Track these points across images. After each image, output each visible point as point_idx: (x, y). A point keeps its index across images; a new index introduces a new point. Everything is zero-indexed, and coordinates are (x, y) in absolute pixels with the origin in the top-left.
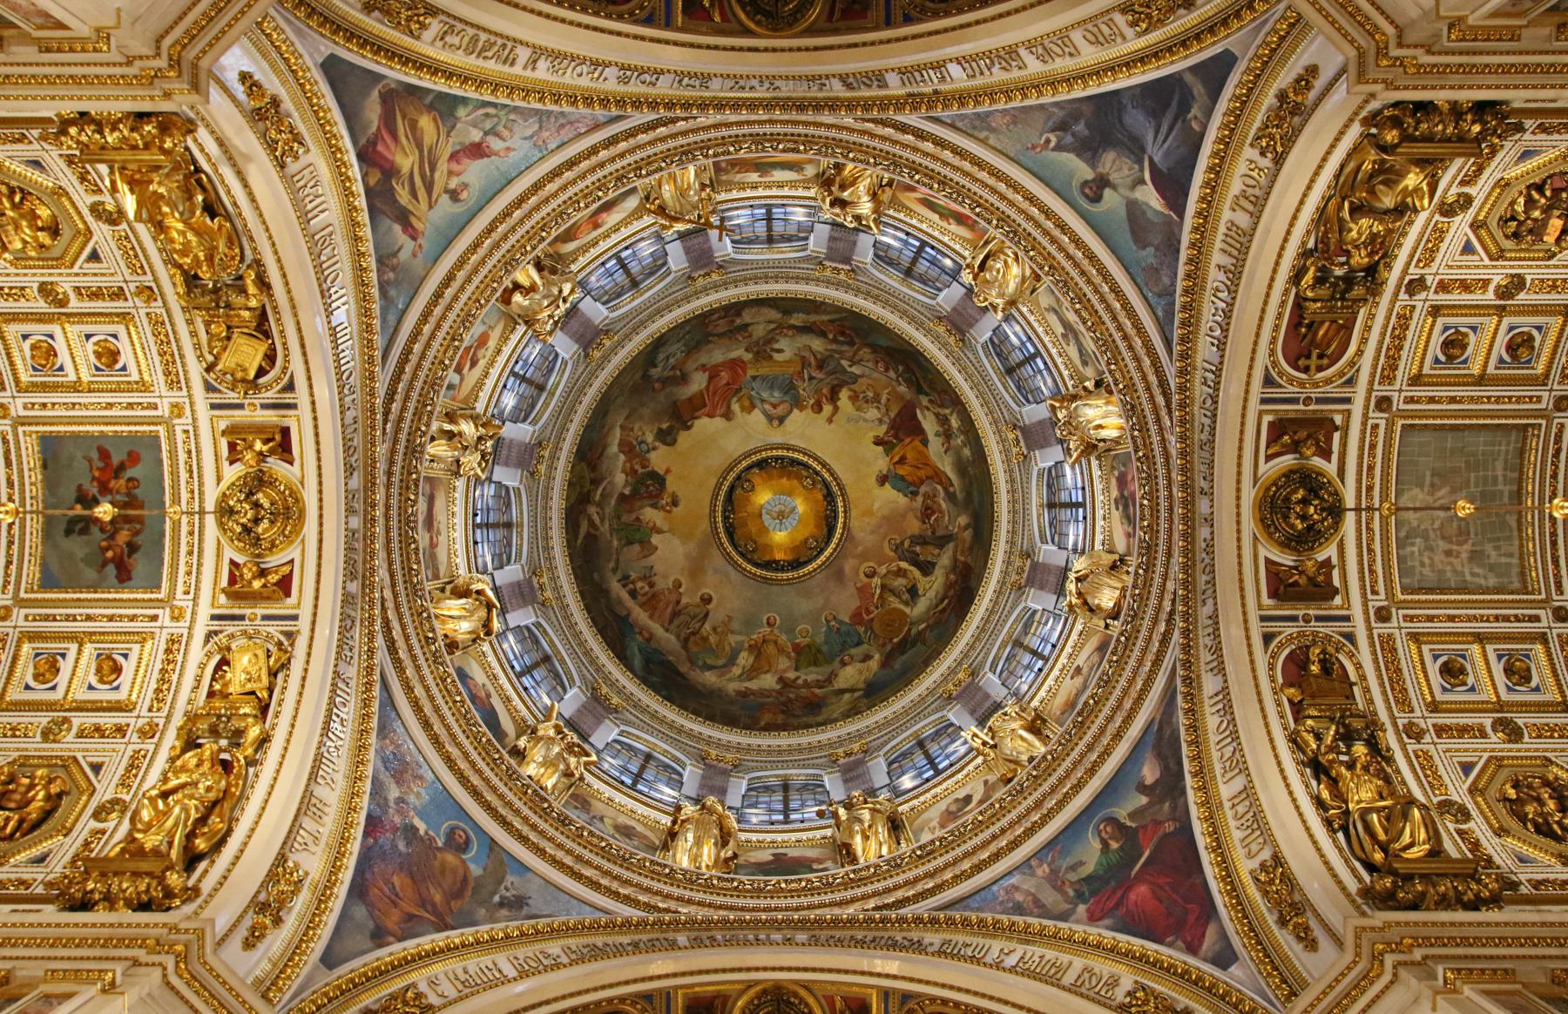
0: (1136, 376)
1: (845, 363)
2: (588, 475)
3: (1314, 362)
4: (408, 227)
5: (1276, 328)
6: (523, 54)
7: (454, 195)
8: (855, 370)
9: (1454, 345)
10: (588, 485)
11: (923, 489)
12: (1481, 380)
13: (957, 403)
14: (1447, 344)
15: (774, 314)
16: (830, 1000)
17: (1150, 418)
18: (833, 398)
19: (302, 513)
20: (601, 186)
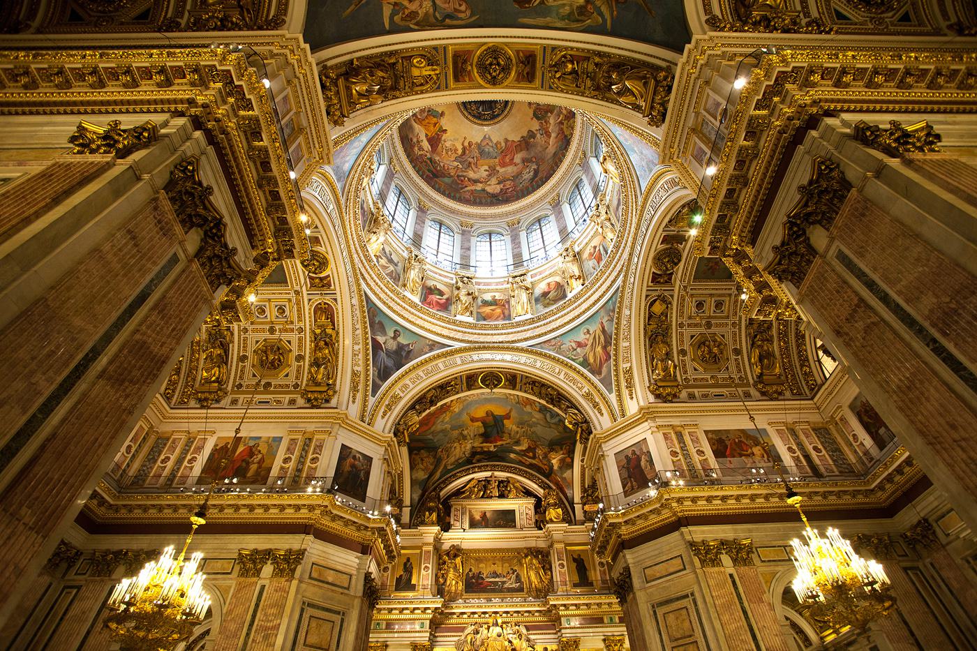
0: (371, 273)
1: (460, 166)
2: (564, 127)
3: (323, 306)
4: (603, 328)
5: (338, 317)
6: (562, 376)
7: (588, 332)
8: (456, 164)
9: (281, 310)
10: (565, 122)
11: (426, 114)
12: (269, 300)
13: (414, 160)
14: (284, 312)
15: (488, 189)
16: (471, 80)
17: (364, 261)
18: (464, 149)
19: (654, 258)
20: (545, 318)
